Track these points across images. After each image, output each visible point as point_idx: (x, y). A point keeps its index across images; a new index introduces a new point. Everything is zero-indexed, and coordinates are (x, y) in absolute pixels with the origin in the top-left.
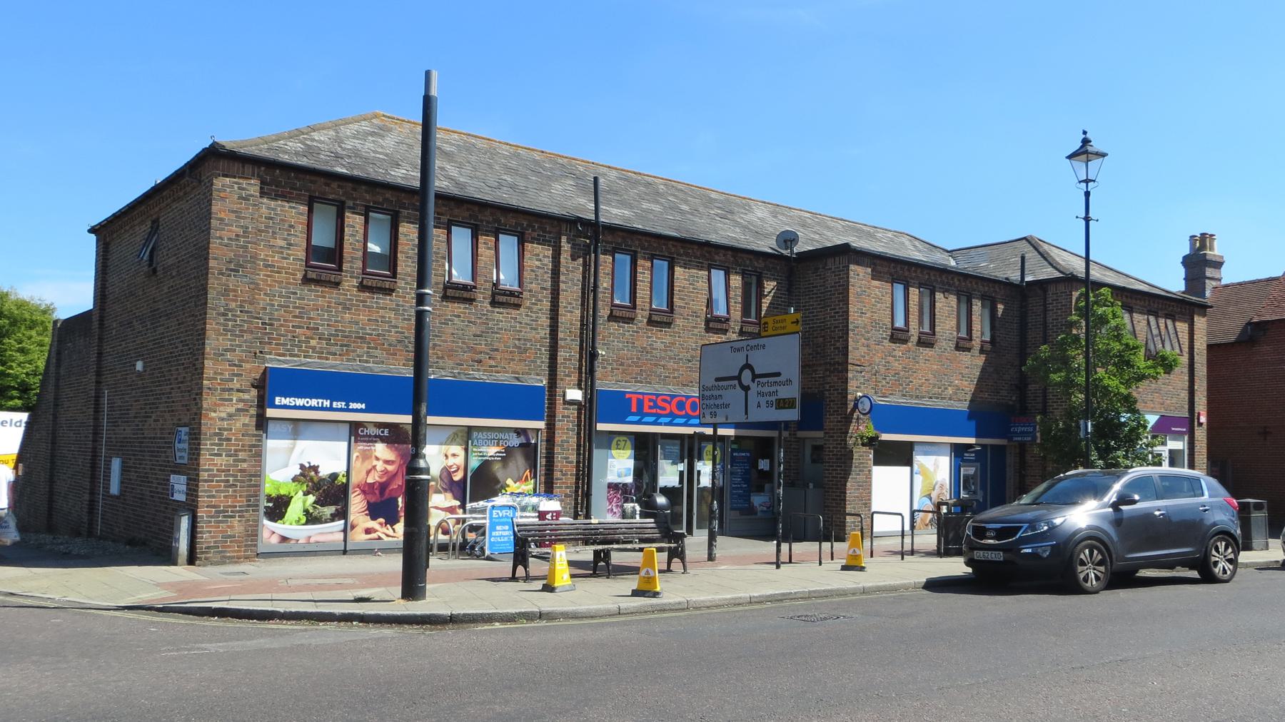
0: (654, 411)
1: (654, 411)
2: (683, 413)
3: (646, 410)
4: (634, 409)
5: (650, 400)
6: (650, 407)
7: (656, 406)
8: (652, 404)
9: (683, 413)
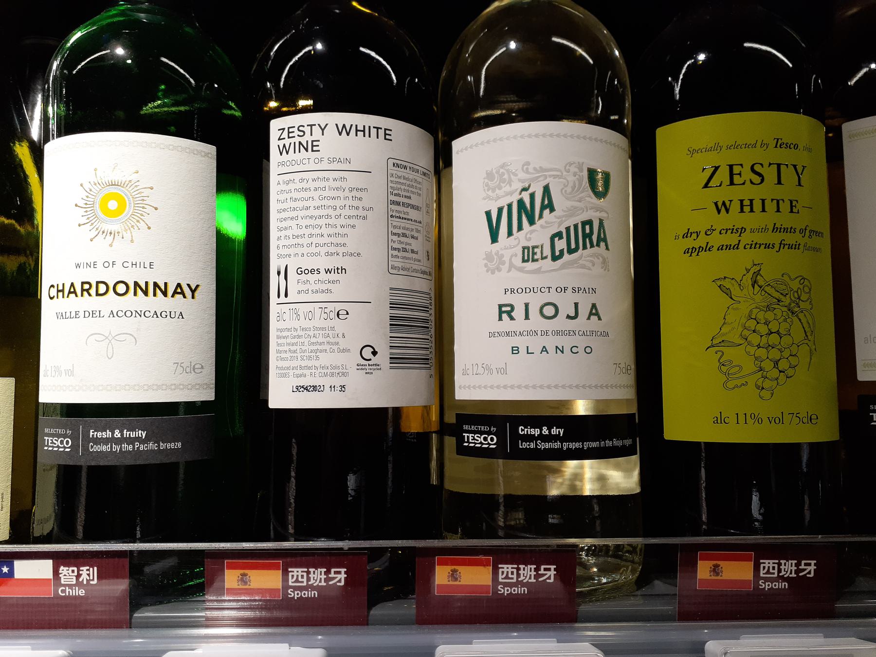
0: (473, 441)
1: (473, 441)
2: (487, 442)
3: (470, 441)
5: (472, 436)
6: (472, 440)
7: (474, 439)
8: (472, 438)
9: (487, 442)
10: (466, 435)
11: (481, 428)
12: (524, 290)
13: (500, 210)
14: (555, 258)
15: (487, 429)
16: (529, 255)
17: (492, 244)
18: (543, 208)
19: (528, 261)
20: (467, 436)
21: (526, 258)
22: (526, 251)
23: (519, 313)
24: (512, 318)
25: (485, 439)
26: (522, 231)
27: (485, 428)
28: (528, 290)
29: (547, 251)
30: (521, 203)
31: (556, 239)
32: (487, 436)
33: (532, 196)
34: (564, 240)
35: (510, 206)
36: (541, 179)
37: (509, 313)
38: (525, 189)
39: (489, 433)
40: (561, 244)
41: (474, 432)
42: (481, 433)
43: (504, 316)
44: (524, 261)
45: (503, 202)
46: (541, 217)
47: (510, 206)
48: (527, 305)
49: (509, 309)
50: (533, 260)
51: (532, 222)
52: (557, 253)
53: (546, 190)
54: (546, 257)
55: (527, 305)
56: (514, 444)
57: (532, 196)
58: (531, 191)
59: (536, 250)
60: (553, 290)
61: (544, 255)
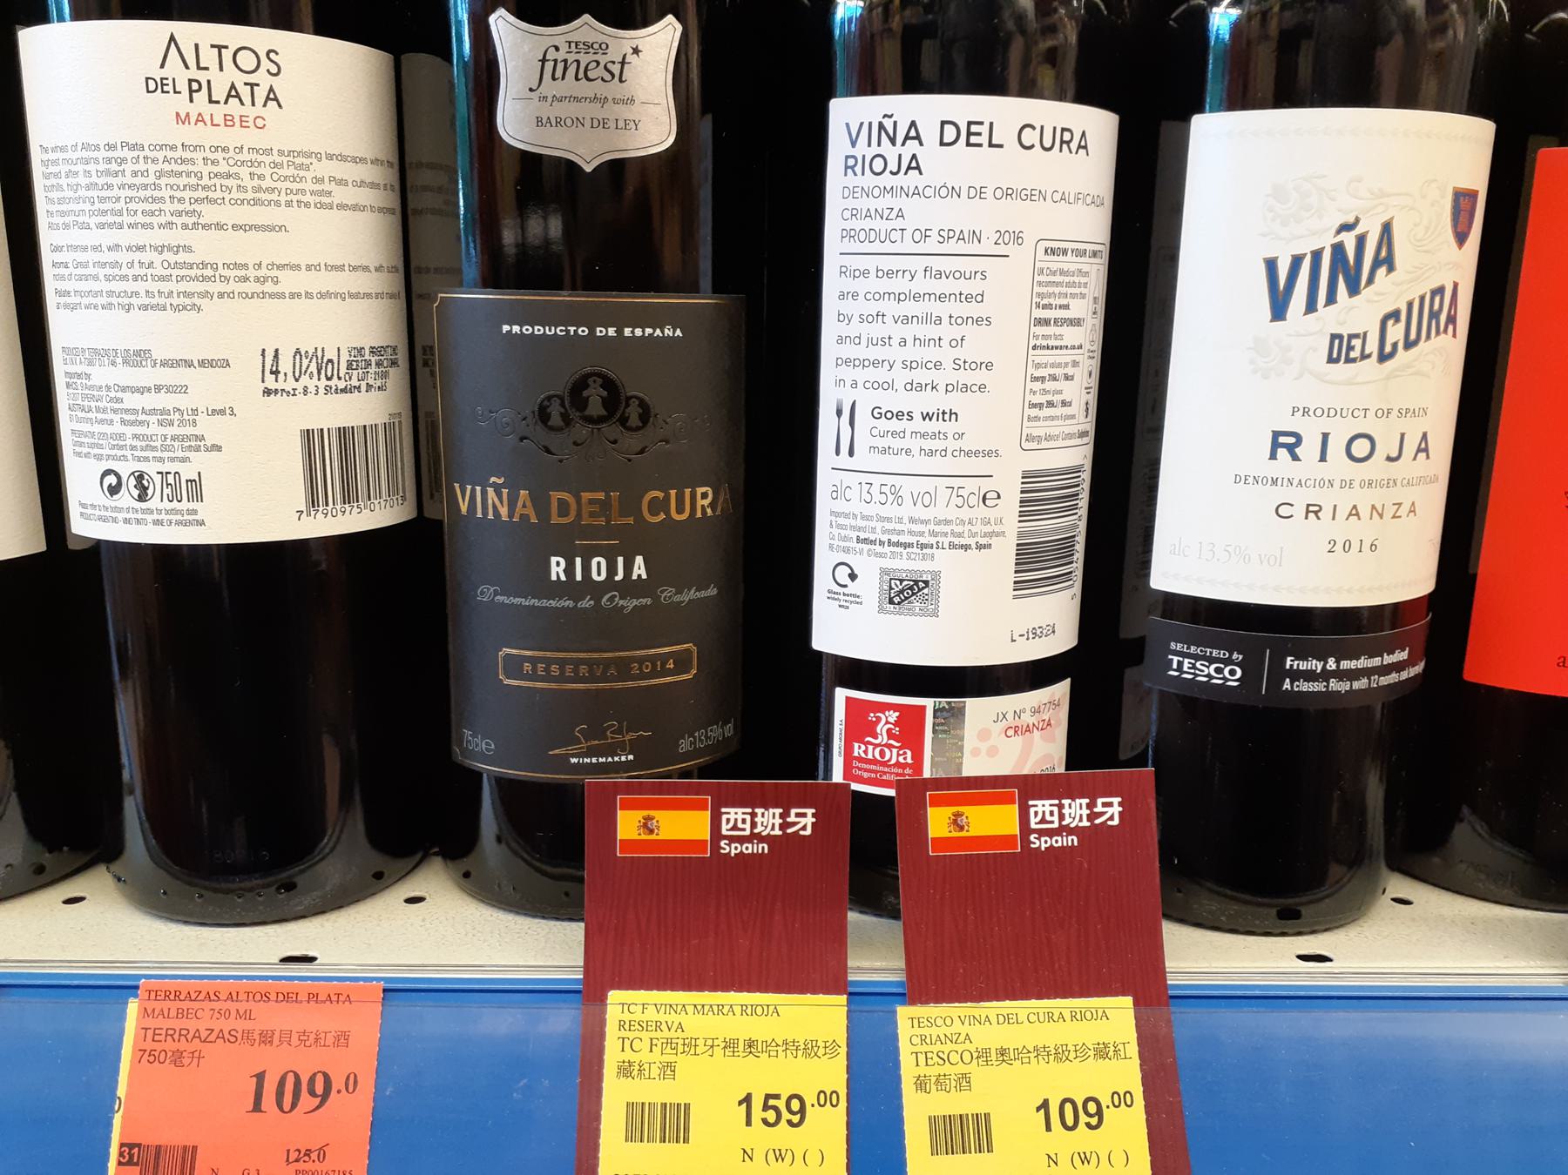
0: (1192, 671)
1: (1192, 671)
2: (1221, 676)
3: (1185, 669)
4: (1175, 666)
5: (1189, 663)
6: (1189, 668)
7: (1194, 667)
8: (1191, 666)
9: (1221, 676)
10: (1176, 659)
11: (1211, 653)
12: (1328, 413)
13: (1297, 261)
14: (1383, 357)
15: (1224, 654)
16: (1341, 349)
17: (1271, 321)
18: (1377, 264)
19: (1337, 361)
20: (1178, 661)
21: (1335, 355)
22: (1337, 342)
23: (1309, 449)
24: (1295, 458)
25: (1218, 670)
26: (1335, 305)
27: (1219, 653)
28: (1332, 413)
29: (1372, 346)
30: (1338, 249)
31: (1390, 323)
32: (1222, 666)
33: (1361, 241)
34: (1402, 325)
35: (1317, 255)
36: (1380, 209)
37: (1291, 449)
38: (1346, 227)
39: (1228, 662)
40: (1395, 332)
41: (1196, 657)
42: (1211, 660)
43: (1282, 453)
44: (1331, 360)
45: (1306, 248)
46: (1370, 281)
47: (1317, 255)
48: (1325, 436)
49: (1292, 440)
50: (1349, 360)
51: (1354, 290)
52: (1388, 349)
53: (1387, 229)
54: (1369, 356)
55: (1325, 436)
56: (1276, 680)
57: (1361, 241)
58: (1358, 230)
59: (1354, 342)
60: (1371, 414)
61: (1367, 352)
